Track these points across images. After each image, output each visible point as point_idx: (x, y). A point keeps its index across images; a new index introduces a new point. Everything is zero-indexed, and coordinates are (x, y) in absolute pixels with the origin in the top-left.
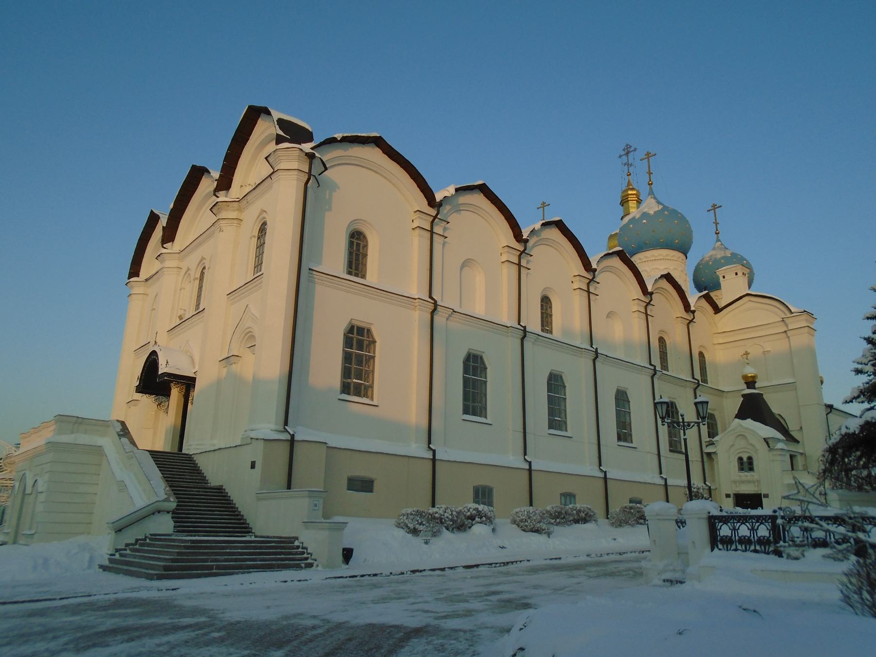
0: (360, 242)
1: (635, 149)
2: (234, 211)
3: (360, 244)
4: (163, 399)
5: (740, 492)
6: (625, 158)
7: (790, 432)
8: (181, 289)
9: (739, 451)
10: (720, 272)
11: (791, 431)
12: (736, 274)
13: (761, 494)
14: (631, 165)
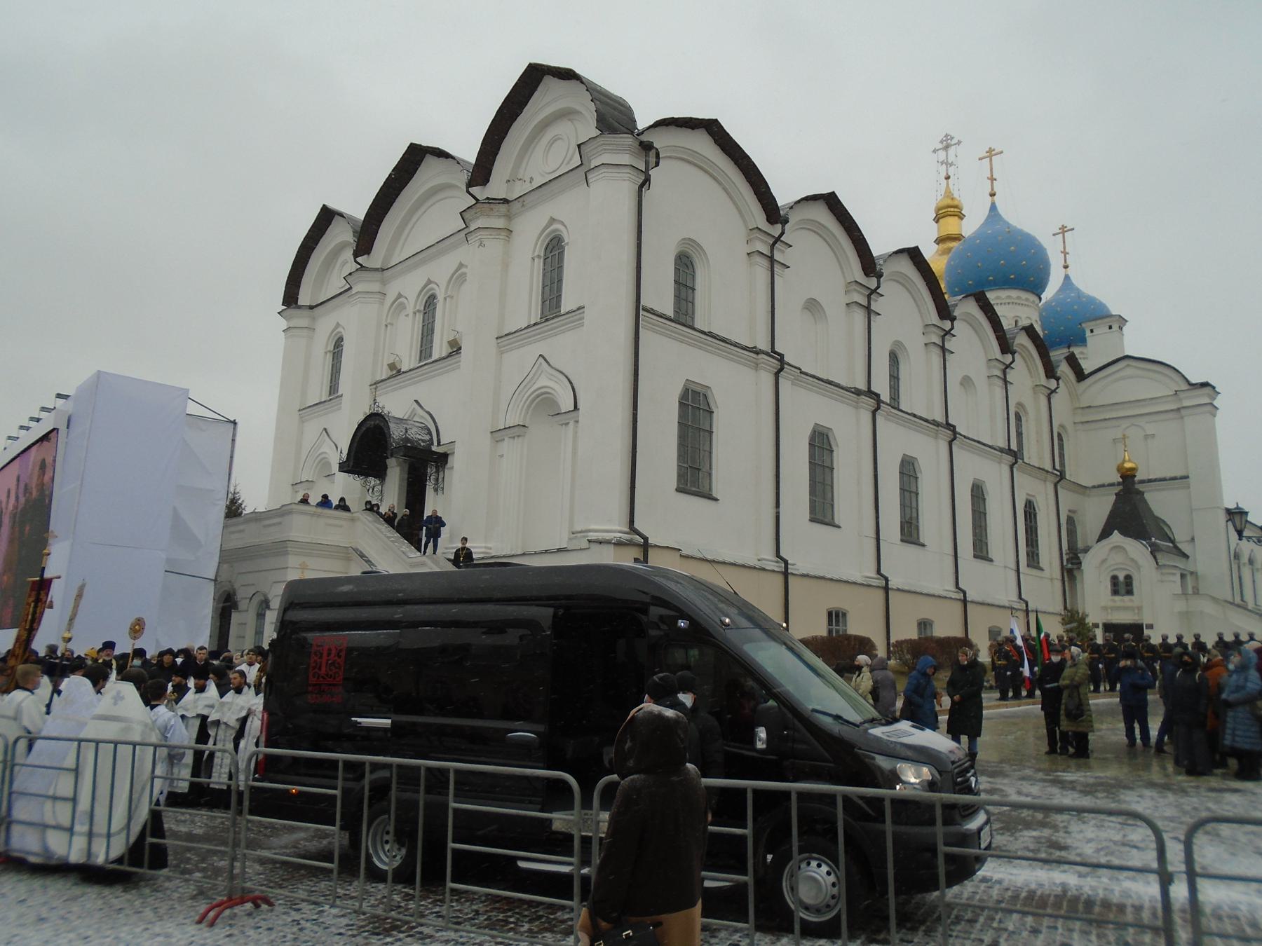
1: (959, 143)
2: (499, 217)
4: (373, 481)
5: (1114, 622)
6: (942, 155)
7: (1178, 545)
8: (386, 326)
9: (1113, 568)
10: (1087, 327)
11: (1180, 542)
12: (1110, 327)
13: (1142, 624)
14: (952, 164)
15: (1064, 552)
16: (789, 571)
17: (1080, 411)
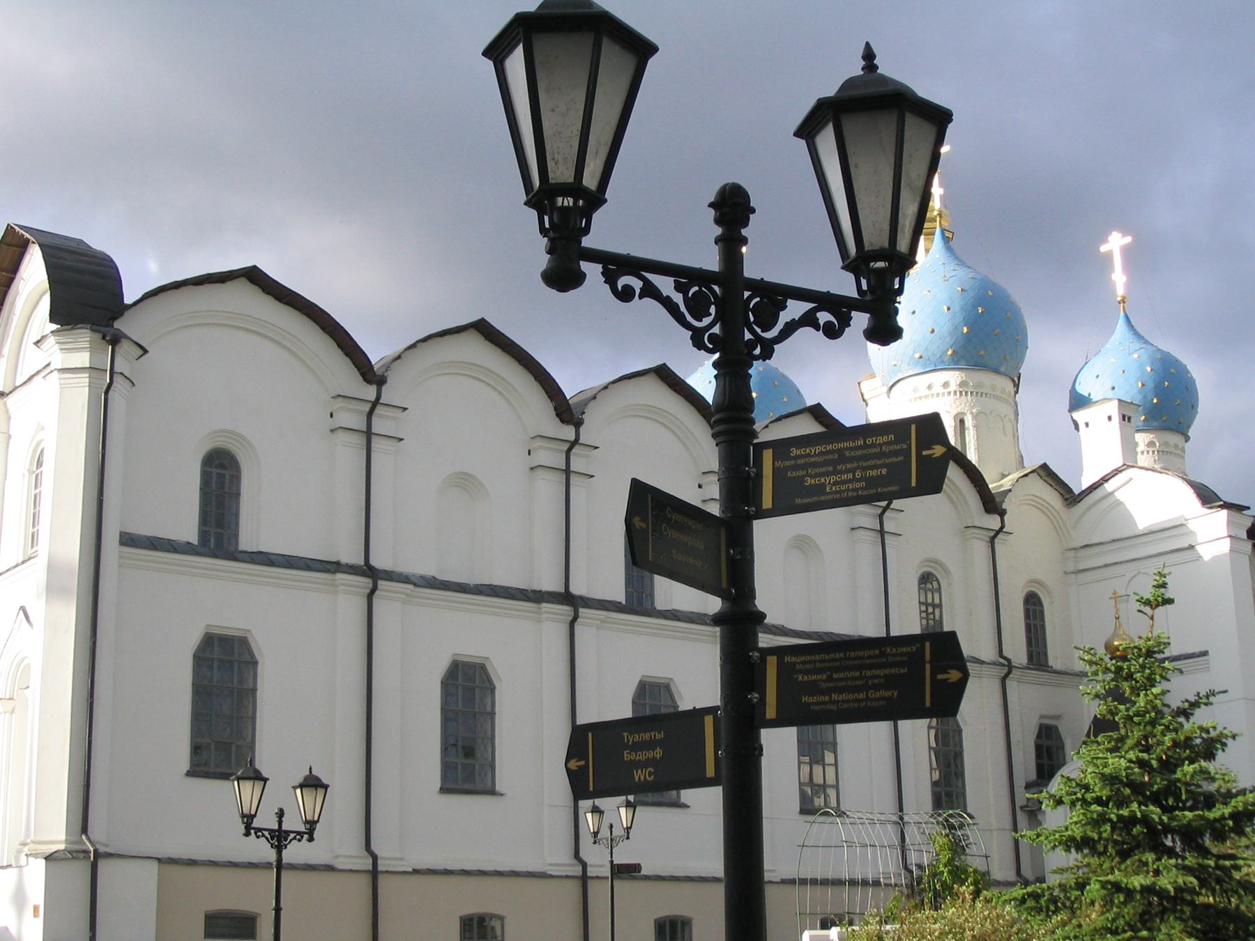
0: (223, 472)
3: (224, 475)
12: (1110, 418)
15: (1020, 783)
16: (380, 868)
17: (1072, 554)
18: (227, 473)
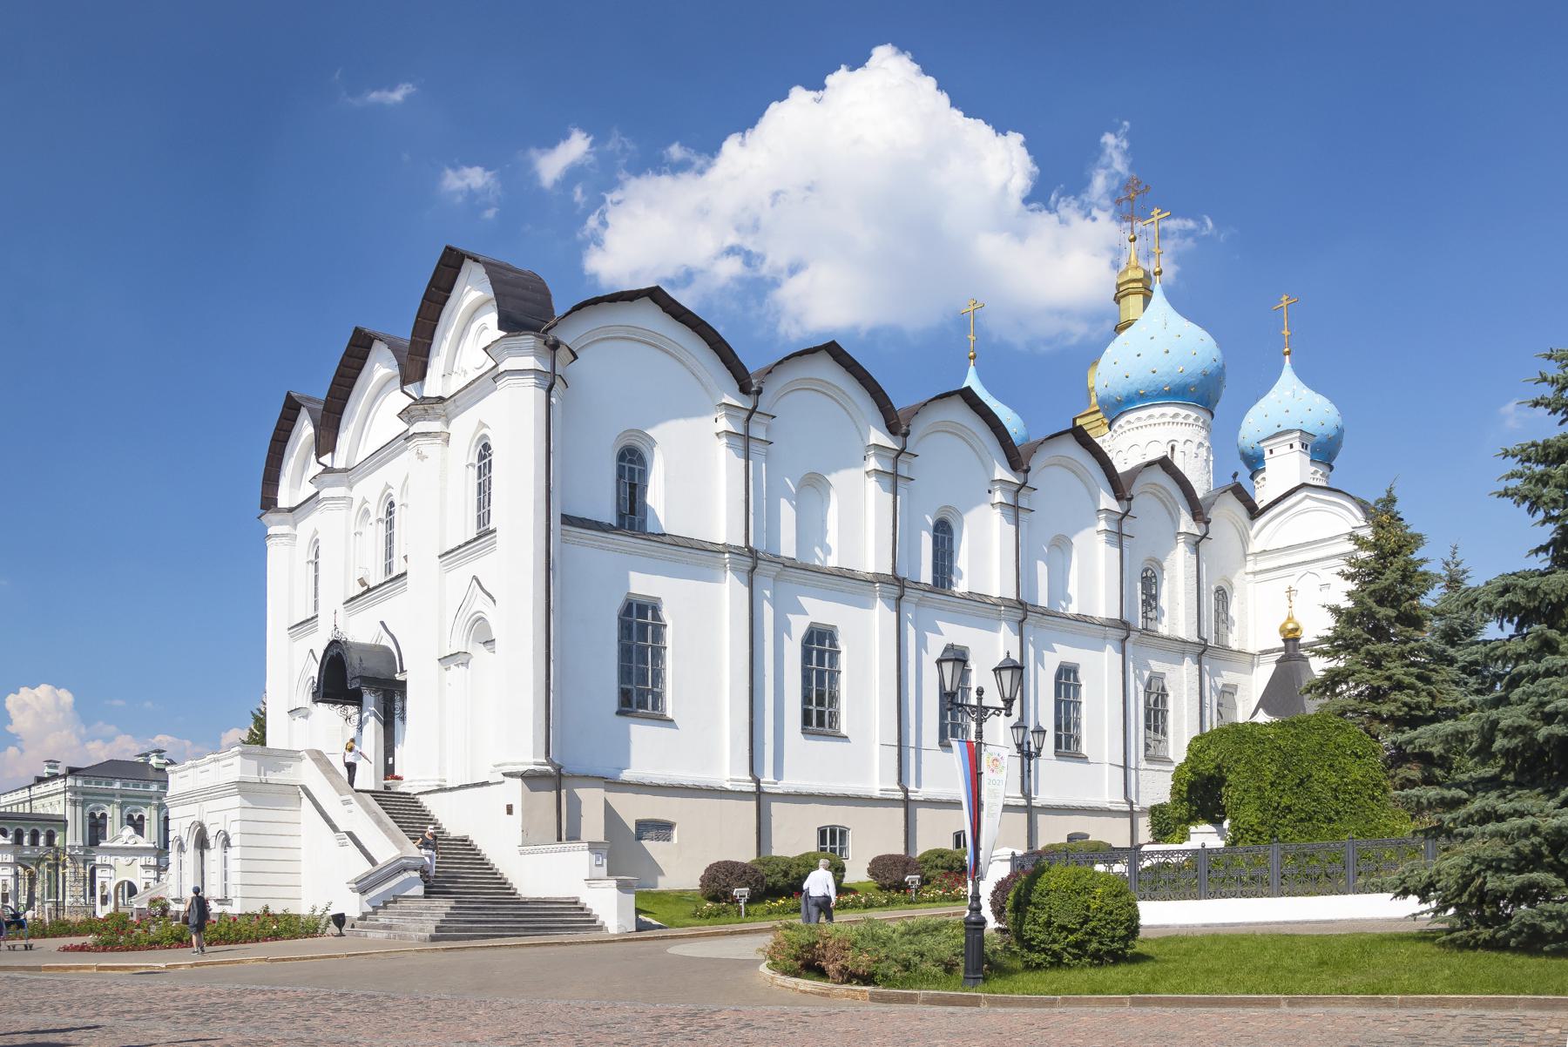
18: (637, 467)
